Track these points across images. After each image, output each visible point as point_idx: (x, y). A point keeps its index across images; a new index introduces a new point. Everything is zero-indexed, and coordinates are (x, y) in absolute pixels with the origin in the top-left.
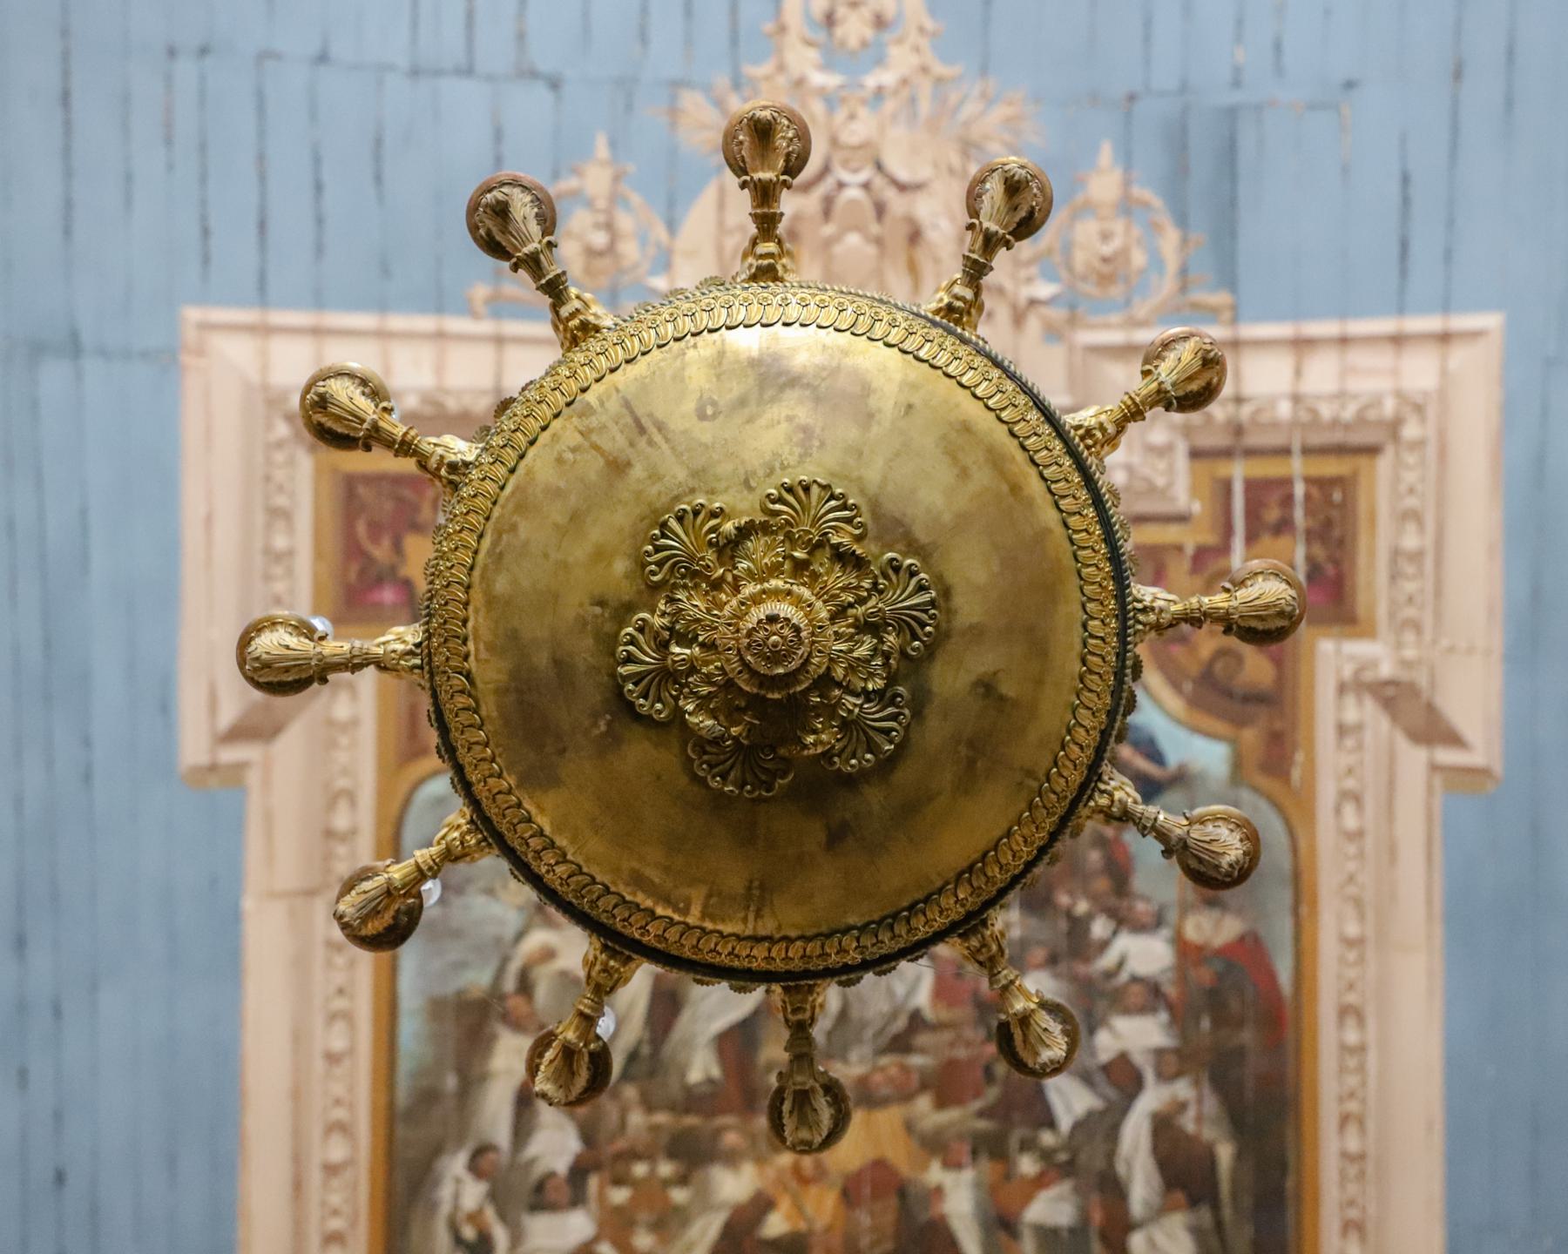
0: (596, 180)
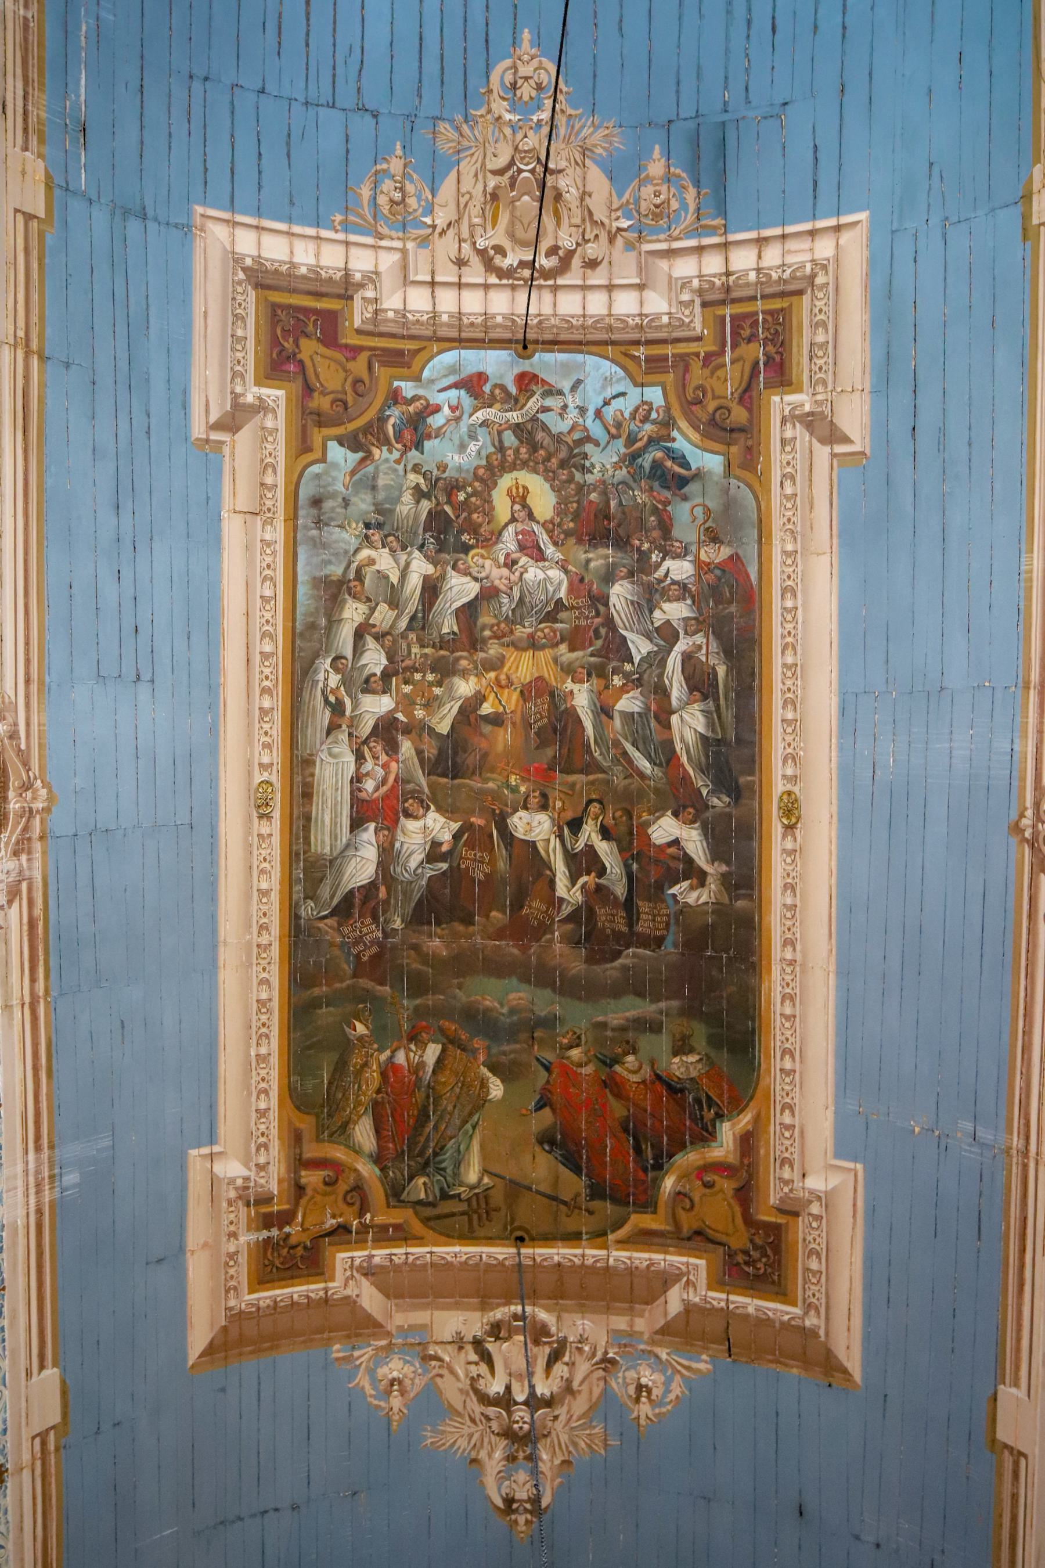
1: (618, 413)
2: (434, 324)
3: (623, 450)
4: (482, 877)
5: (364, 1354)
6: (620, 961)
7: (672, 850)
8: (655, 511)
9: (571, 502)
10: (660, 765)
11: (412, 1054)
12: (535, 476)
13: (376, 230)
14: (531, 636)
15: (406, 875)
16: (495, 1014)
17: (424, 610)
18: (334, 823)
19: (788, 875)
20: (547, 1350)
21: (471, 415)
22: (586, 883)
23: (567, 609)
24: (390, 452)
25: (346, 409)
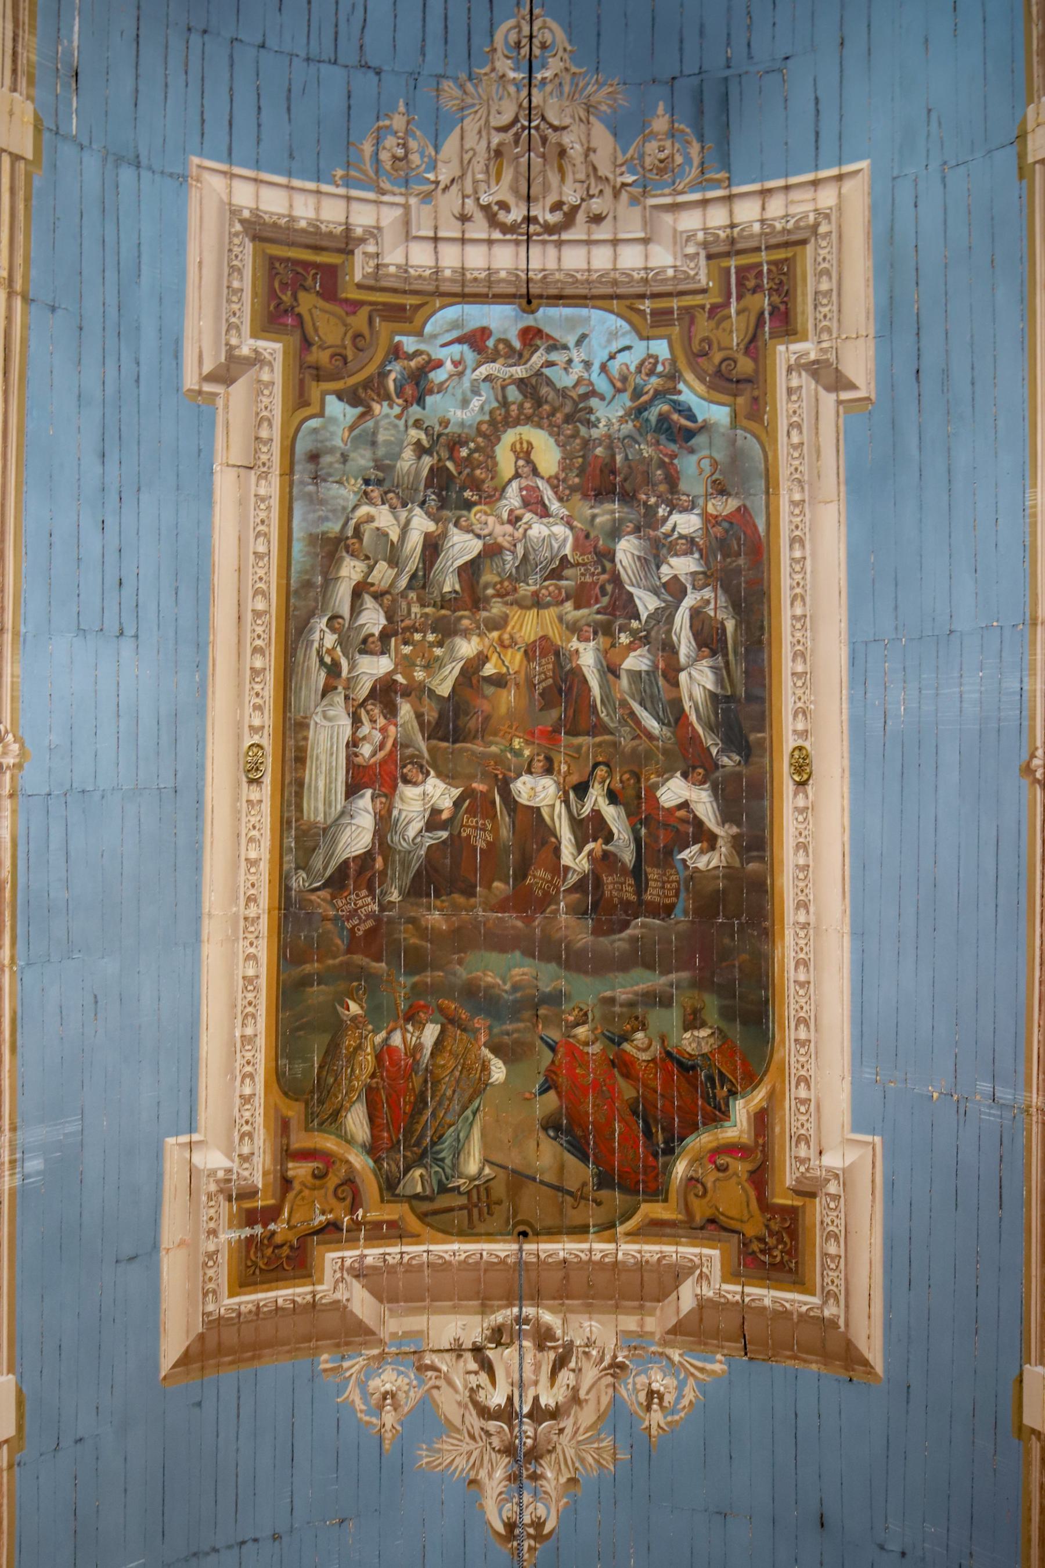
0: (398, 122)
1: (624, 368)
2: (437, 280)
3: (629, 404)
4: (484, 846)
5: (354, 1365)
6: (629, 932)
7: (681, 813)
8: (662, 464)
10: (669, 725)
11: (409, 1036)
13: (378, 186)
14: (536, 594)
15: (404, 844)
16: (497, 991)
17: (424, 569)
18: (328, 790)
19: (800, 834)
20: (552, 1355)
21: (474, 370)
22: (593, 850)
23: (572, 566)
24: (391, 407)
25: (346, 363)
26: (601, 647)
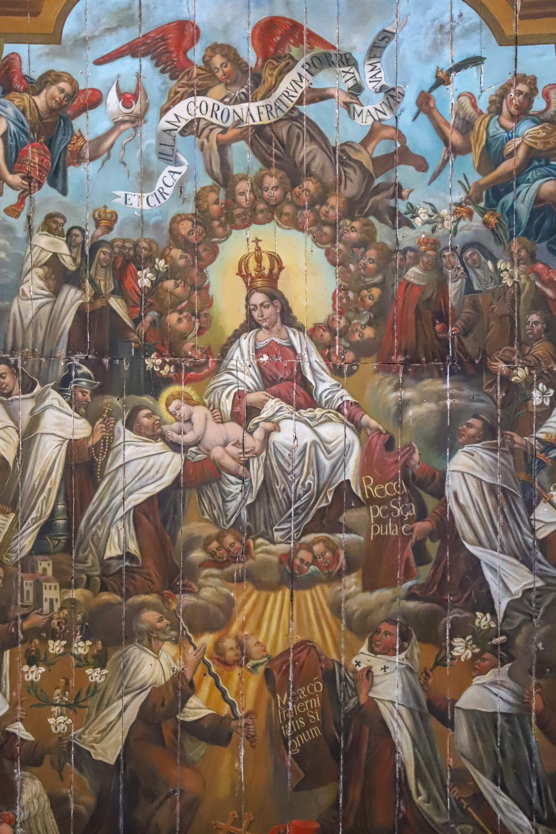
1: (466, 101)
3: (475, 178)
9: (368, 287)
12: (295, 234)
17: (68, 512)
21: (164, 111)
23: (360, 504)
26: (417, 666)
